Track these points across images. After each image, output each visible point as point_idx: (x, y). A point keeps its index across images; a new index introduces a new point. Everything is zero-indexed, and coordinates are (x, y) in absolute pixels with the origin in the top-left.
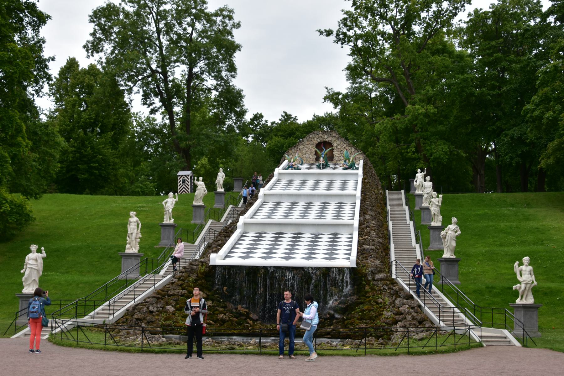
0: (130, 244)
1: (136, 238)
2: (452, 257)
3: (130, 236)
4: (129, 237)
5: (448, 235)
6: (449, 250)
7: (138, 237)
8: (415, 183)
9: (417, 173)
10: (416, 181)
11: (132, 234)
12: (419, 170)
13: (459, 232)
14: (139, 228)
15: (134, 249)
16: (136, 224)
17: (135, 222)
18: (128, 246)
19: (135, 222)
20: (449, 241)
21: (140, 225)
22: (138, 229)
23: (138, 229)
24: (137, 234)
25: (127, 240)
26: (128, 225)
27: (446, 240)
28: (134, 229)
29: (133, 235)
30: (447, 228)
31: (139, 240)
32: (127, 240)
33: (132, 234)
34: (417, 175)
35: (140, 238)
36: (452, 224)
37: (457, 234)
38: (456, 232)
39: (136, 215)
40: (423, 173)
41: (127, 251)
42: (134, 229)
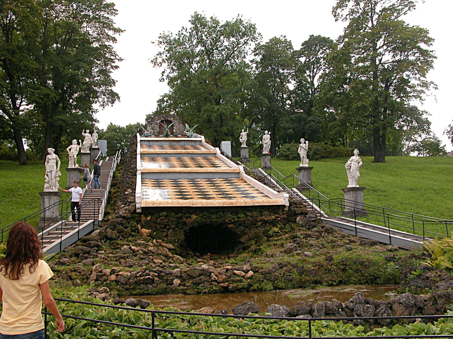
0: (48, 182)
1: (56, 177)
2: (357, 186)
3: (49, 174)
4: (47, 175)
5: (352, 165)
6: (354, 179)
7: (58, 175)
8: (240, 140)
9: (242, 132)
10: (241, 138)
11: (51, 171)
12: (243, 130)
13: (361, 163)
14: (59, 166)
15: (54, 188)
16: (55, 161)
17: (54, 159)
18: (46, 185)
19: (54, 159)
20: (354, 172)
21: (59, 163)
22: (57, 167)
23: (57, 167)
24: (57, 172)
25: (46, 179)
26: (46, 163)
27: (351, 171)
28: (53, 166)
29: (53, 173)
30: (350, 159)
31: (58, 179)
32: (46, 179)
33: (51, 171)
34: (241, 133)
35: (59, 176)
36: (354, 155)
37: (360, 164)
38: (359, 163)
39: (55, 153)
40: (246, 132)
41: (46, 190)
42: (53, 166)
